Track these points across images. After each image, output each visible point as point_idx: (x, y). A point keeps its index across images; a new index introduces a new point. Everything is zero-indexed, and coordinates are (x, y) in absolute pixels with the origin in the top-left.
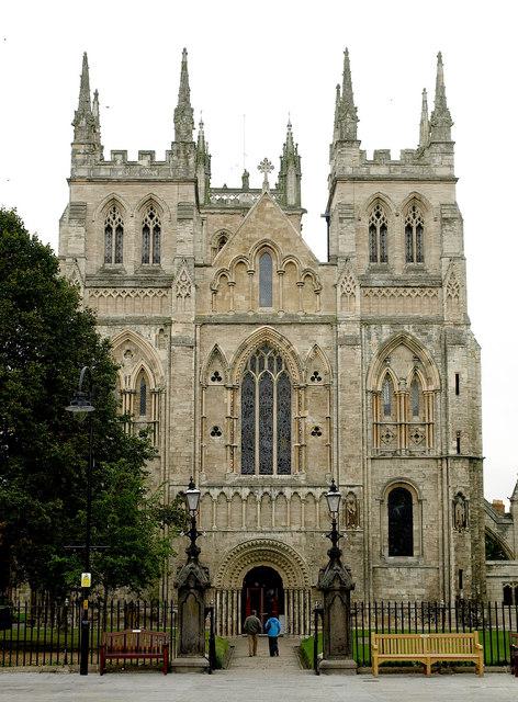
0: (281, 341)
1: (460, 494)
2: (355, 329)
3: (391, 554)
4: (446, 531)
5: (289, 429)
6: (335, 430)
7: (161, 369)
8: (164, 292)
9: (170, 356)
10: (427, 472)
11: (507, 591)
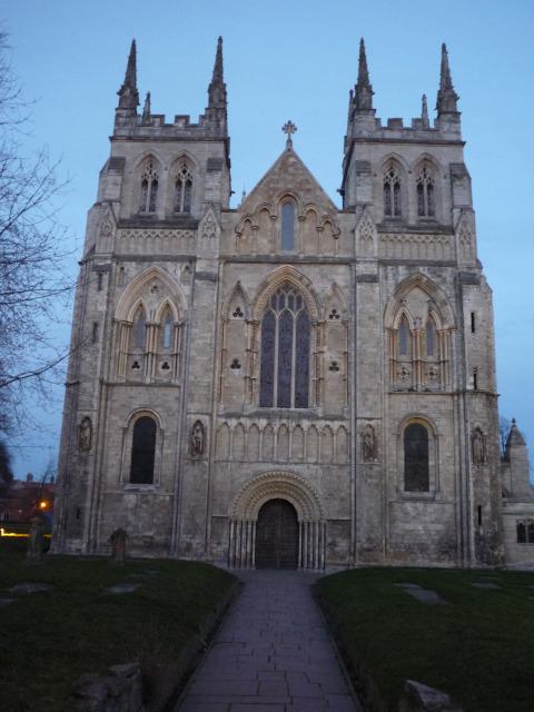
0: (300, 279)
1: (478, 429)
2: (373, 269)
3: (406, 489)
4: (464, 466)
5: (308, 360)
6: (353, 365)
7: (185, 302)
8: (191, 233)
9: (193, 290)
10: (443, 407)
11: (520, 528)
